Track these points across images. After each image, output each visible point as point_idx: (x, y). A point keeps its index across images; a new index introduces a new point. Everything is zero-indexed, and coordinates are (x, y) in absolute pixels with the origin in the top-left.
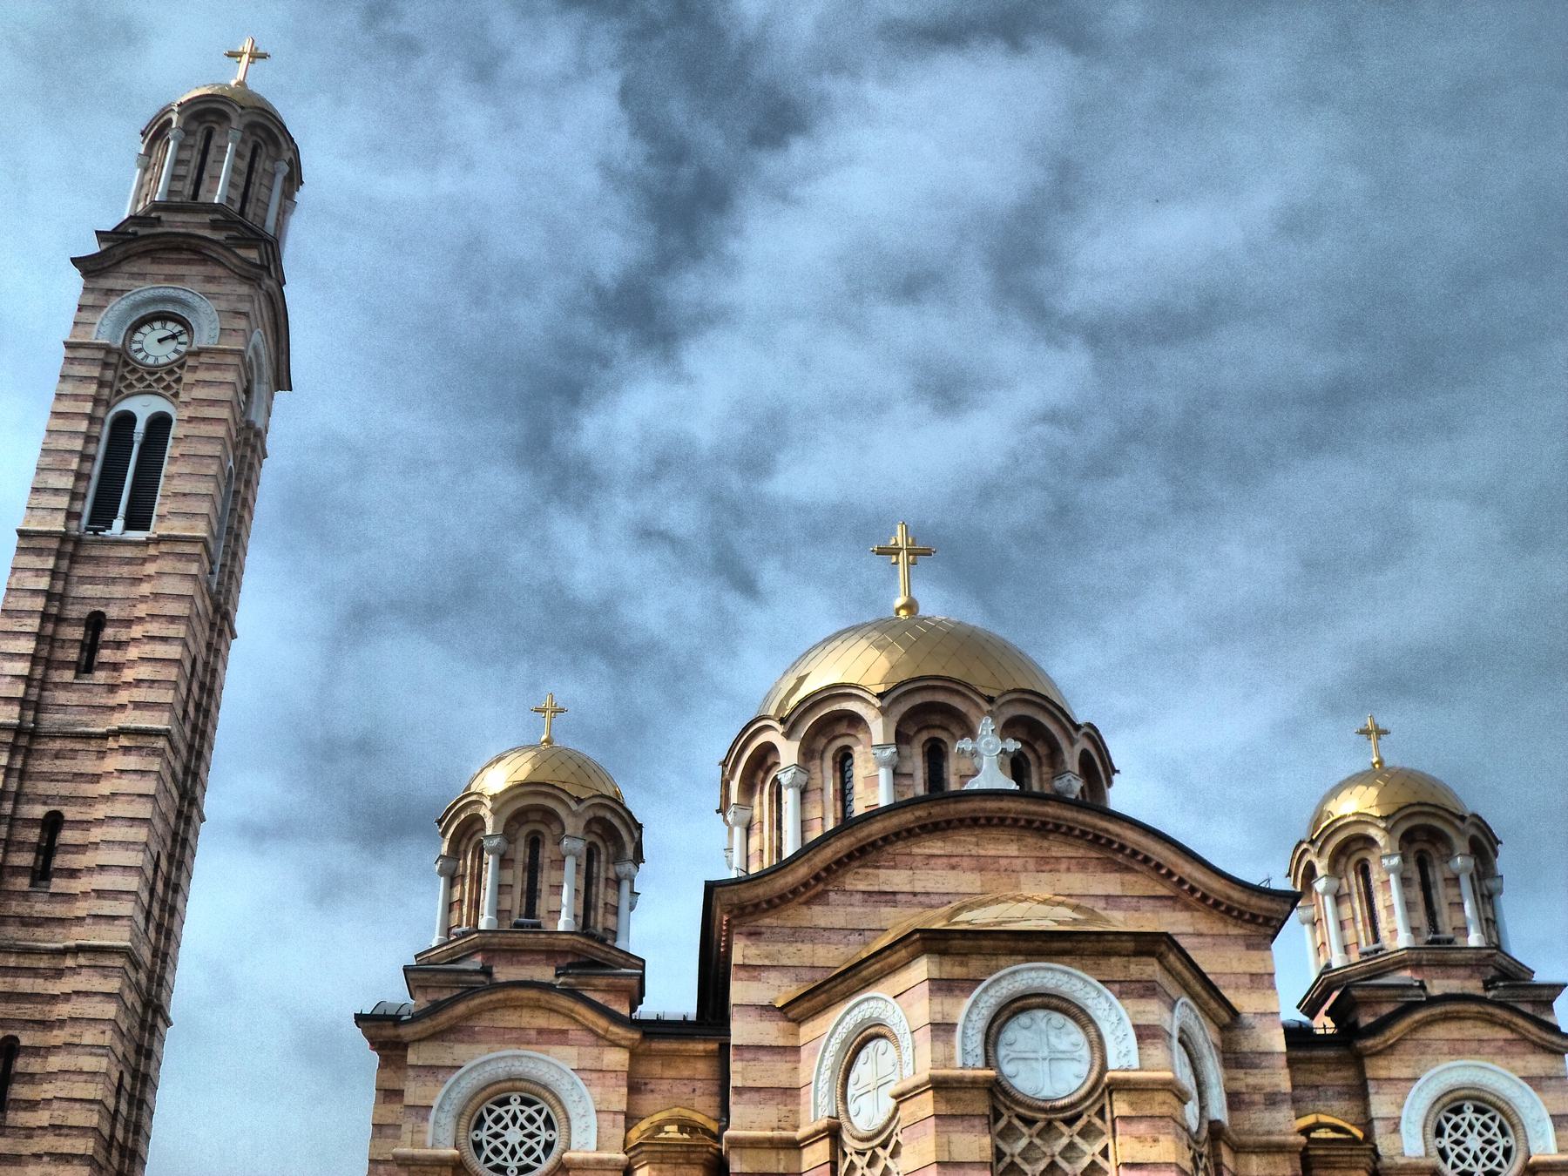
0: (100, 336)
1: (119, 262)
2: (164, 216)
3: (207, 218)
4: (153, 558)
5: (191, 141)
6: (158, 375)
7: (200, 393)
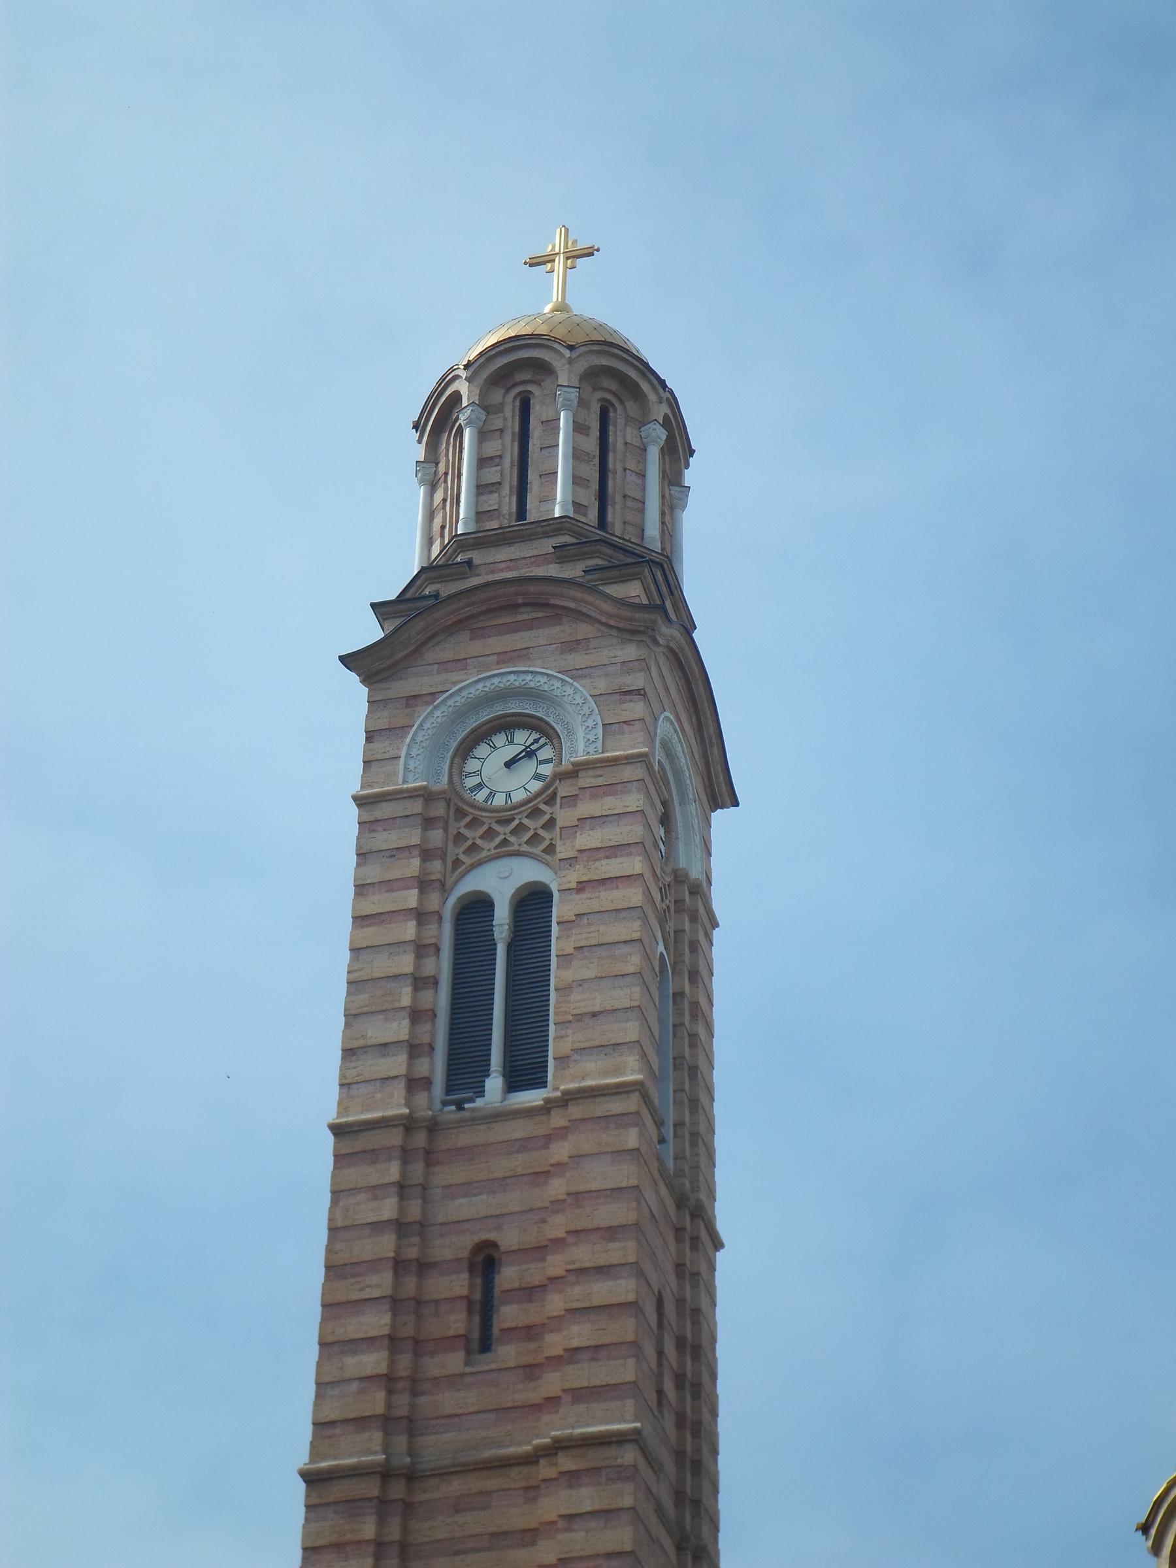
0: (411, 776)
2: (478, 557)
3: (546, 546)
4: (562, 1133)
6: (516, 822)
7: (589, 839)
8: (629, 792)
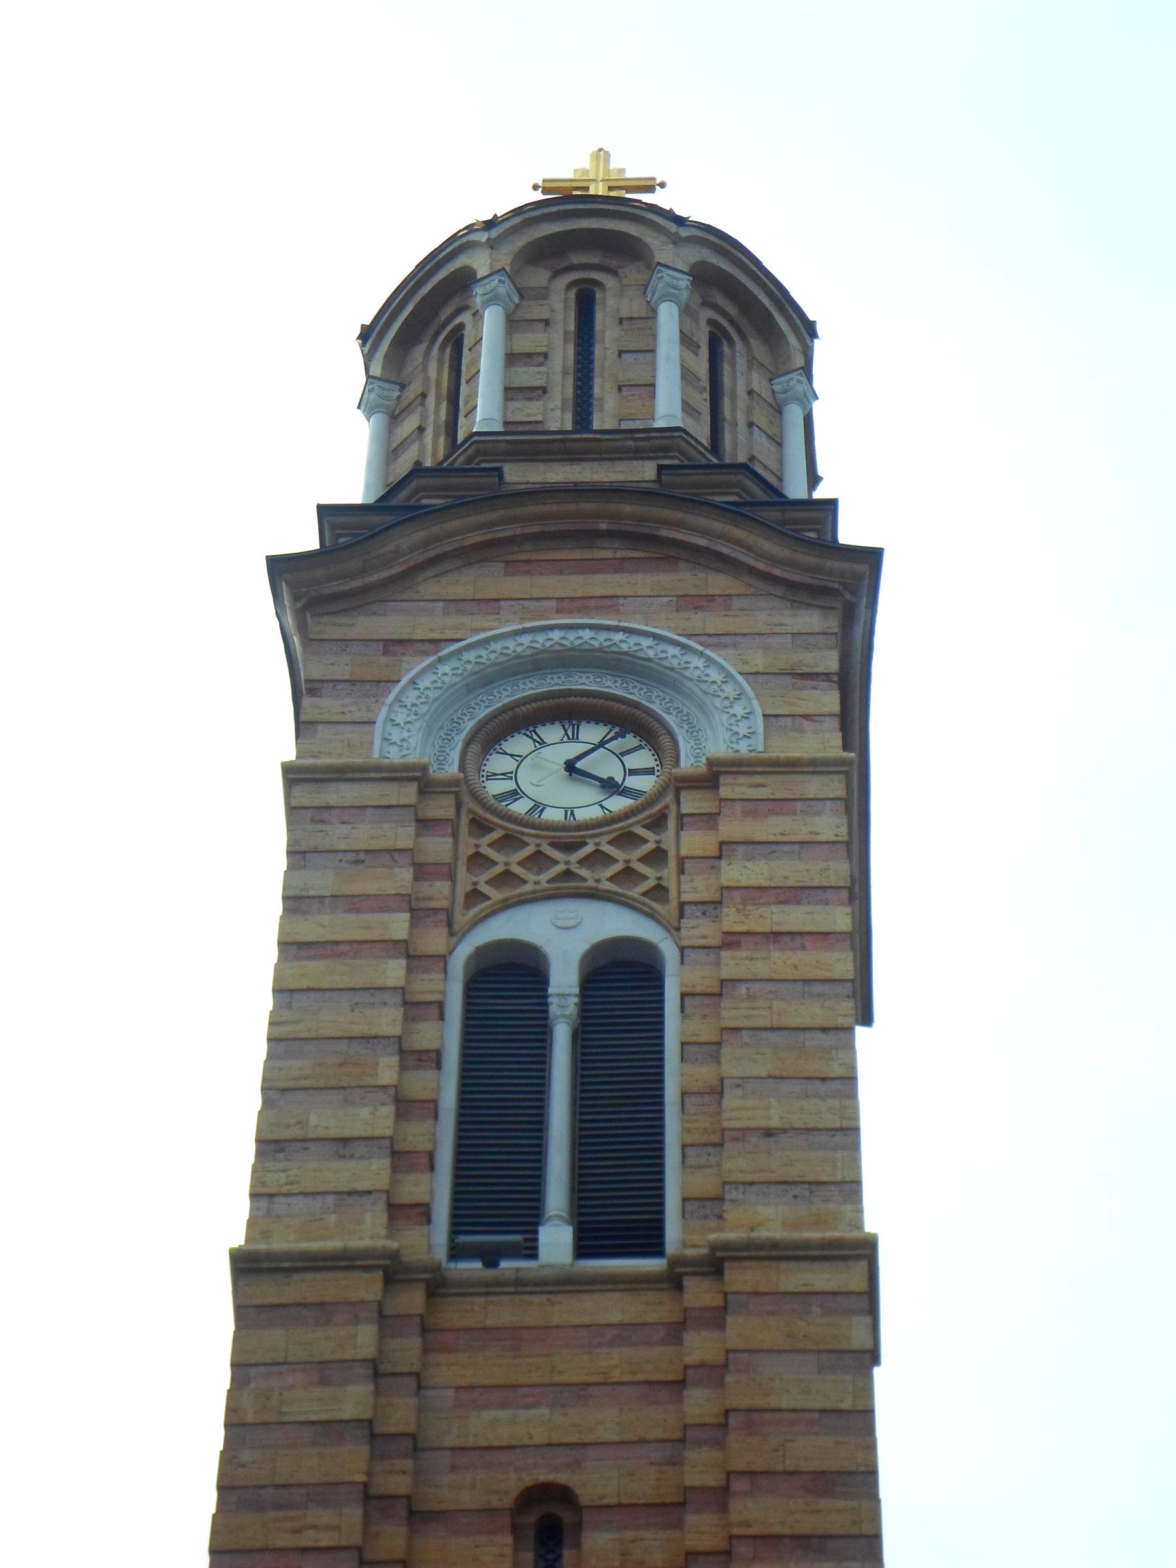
1: (408, 576)
5: (538, 311)
8: (819, 813)
